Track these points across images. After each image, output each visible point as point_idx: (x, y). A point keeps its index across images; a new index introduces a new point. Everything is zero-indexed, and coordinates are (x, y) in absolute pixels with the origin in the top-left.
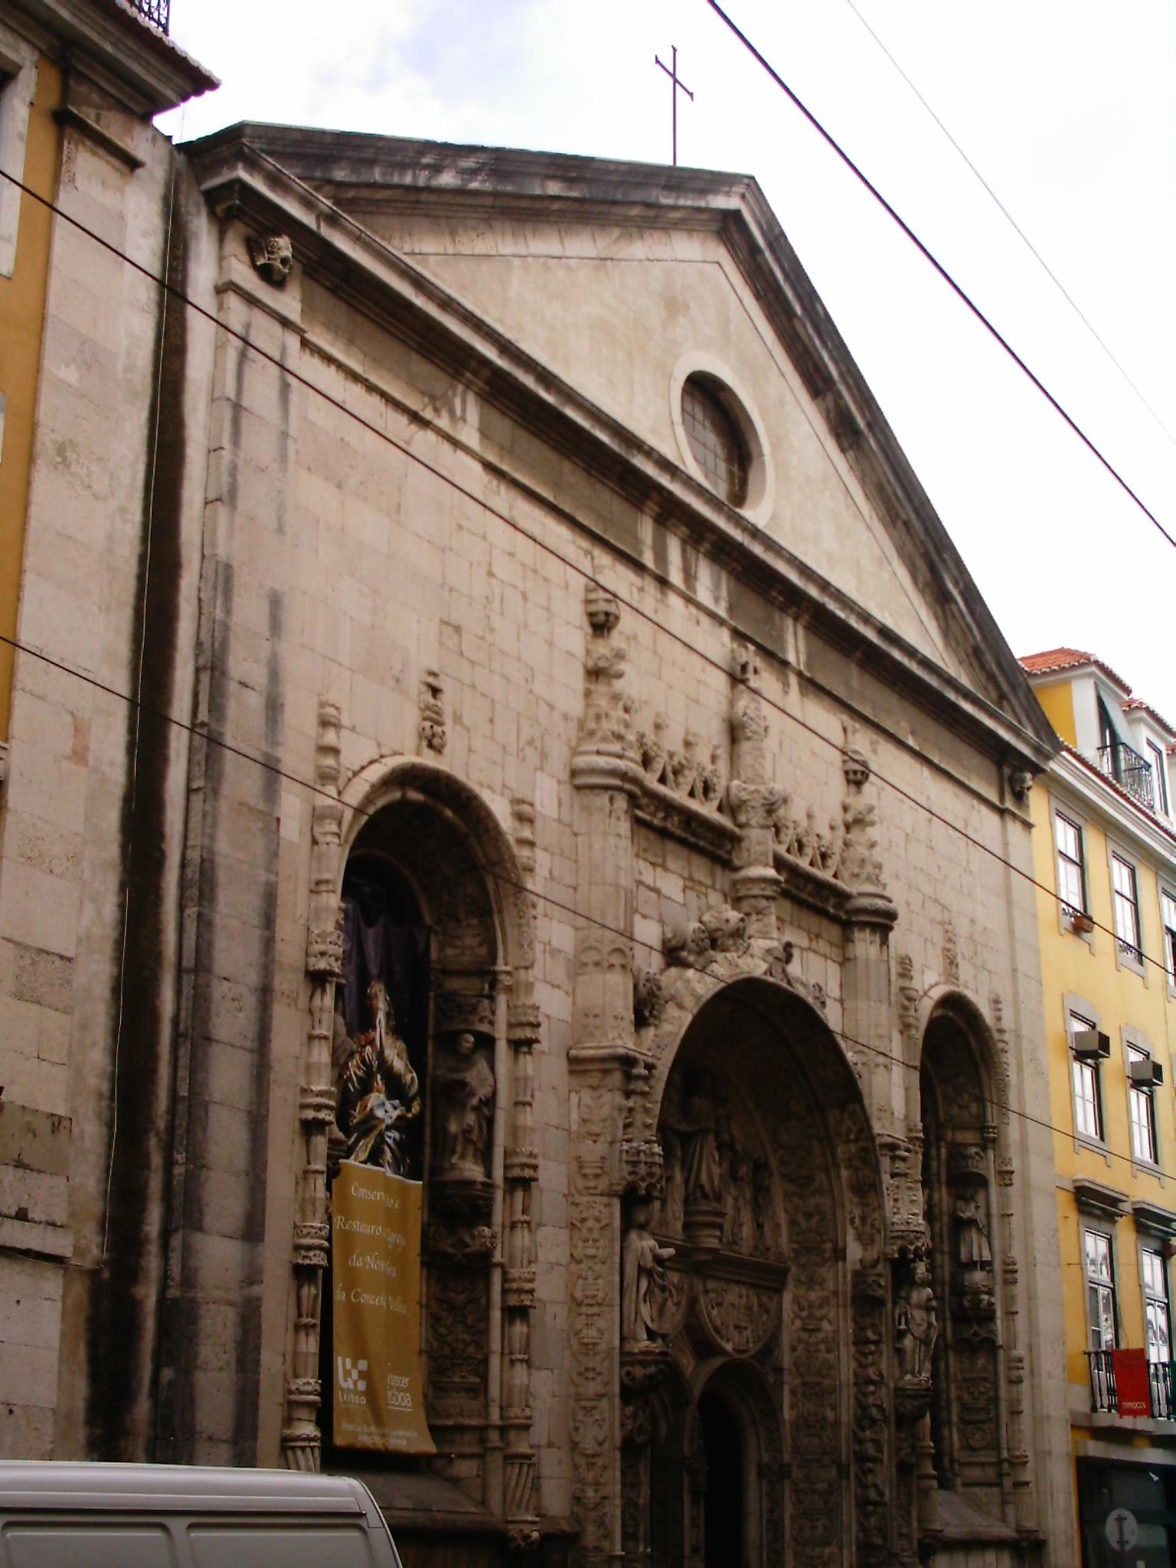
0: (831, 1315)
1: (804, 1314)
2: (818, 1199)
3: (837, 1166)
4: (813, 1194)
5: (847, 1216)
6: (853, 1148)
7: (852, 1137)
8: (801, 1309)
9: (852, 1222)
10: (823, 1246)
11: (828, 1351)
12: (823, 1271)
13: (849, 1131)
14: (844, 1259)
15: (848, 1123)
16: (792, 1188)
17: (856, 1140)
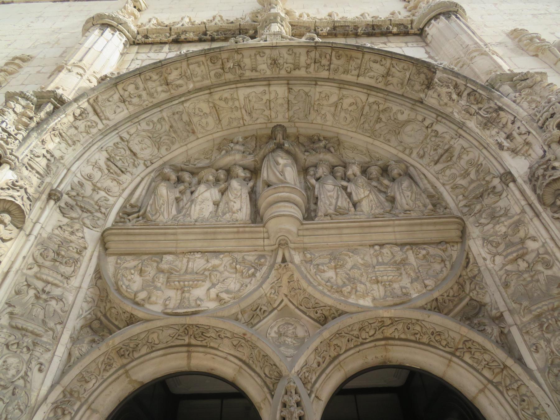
0: (532, 232)
1: (502, 247)
2: (465, 158)
3: (461, 126)
4: (459, 157)
5: (495, 148)
6: (463, 102)
7: (455, 96)
8: (498, 244)
9: (501, 147)
10: (491, 185)
11: (548, 265)
12: (502, 203)
13: (449, 94)
14: (514, 181)
15: (444, 90)
16: (439, 166)
17: (459, 95)
